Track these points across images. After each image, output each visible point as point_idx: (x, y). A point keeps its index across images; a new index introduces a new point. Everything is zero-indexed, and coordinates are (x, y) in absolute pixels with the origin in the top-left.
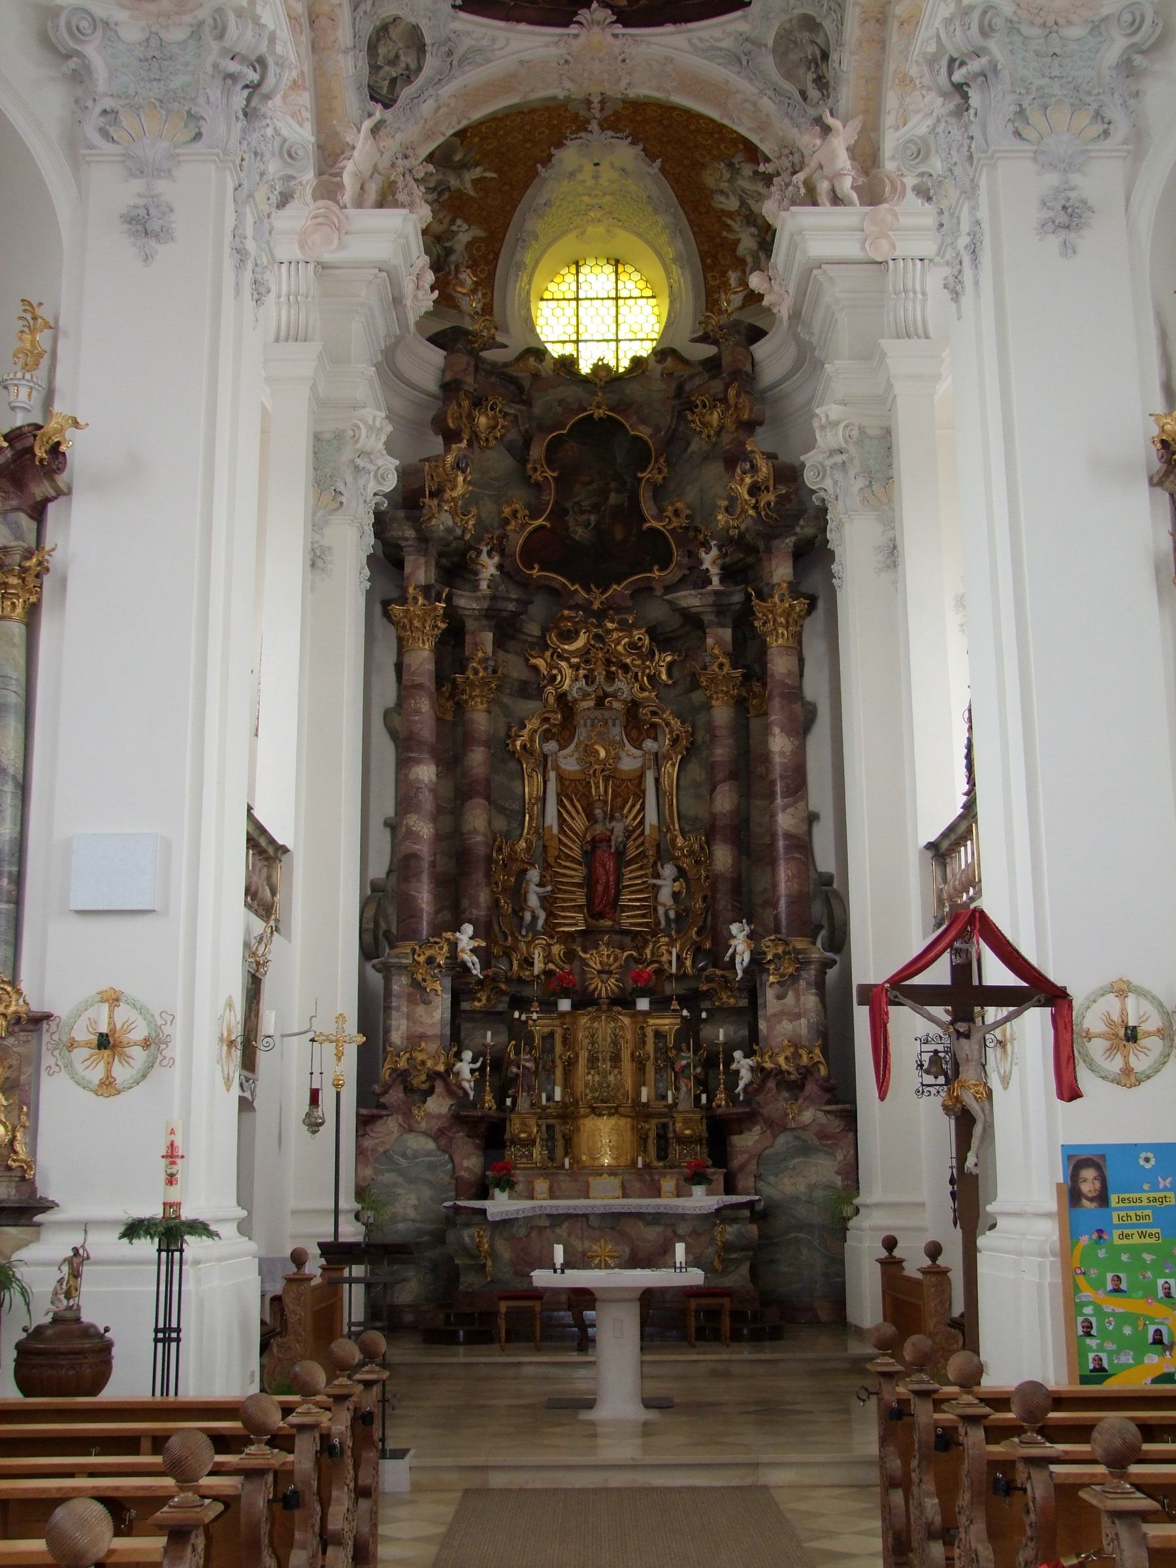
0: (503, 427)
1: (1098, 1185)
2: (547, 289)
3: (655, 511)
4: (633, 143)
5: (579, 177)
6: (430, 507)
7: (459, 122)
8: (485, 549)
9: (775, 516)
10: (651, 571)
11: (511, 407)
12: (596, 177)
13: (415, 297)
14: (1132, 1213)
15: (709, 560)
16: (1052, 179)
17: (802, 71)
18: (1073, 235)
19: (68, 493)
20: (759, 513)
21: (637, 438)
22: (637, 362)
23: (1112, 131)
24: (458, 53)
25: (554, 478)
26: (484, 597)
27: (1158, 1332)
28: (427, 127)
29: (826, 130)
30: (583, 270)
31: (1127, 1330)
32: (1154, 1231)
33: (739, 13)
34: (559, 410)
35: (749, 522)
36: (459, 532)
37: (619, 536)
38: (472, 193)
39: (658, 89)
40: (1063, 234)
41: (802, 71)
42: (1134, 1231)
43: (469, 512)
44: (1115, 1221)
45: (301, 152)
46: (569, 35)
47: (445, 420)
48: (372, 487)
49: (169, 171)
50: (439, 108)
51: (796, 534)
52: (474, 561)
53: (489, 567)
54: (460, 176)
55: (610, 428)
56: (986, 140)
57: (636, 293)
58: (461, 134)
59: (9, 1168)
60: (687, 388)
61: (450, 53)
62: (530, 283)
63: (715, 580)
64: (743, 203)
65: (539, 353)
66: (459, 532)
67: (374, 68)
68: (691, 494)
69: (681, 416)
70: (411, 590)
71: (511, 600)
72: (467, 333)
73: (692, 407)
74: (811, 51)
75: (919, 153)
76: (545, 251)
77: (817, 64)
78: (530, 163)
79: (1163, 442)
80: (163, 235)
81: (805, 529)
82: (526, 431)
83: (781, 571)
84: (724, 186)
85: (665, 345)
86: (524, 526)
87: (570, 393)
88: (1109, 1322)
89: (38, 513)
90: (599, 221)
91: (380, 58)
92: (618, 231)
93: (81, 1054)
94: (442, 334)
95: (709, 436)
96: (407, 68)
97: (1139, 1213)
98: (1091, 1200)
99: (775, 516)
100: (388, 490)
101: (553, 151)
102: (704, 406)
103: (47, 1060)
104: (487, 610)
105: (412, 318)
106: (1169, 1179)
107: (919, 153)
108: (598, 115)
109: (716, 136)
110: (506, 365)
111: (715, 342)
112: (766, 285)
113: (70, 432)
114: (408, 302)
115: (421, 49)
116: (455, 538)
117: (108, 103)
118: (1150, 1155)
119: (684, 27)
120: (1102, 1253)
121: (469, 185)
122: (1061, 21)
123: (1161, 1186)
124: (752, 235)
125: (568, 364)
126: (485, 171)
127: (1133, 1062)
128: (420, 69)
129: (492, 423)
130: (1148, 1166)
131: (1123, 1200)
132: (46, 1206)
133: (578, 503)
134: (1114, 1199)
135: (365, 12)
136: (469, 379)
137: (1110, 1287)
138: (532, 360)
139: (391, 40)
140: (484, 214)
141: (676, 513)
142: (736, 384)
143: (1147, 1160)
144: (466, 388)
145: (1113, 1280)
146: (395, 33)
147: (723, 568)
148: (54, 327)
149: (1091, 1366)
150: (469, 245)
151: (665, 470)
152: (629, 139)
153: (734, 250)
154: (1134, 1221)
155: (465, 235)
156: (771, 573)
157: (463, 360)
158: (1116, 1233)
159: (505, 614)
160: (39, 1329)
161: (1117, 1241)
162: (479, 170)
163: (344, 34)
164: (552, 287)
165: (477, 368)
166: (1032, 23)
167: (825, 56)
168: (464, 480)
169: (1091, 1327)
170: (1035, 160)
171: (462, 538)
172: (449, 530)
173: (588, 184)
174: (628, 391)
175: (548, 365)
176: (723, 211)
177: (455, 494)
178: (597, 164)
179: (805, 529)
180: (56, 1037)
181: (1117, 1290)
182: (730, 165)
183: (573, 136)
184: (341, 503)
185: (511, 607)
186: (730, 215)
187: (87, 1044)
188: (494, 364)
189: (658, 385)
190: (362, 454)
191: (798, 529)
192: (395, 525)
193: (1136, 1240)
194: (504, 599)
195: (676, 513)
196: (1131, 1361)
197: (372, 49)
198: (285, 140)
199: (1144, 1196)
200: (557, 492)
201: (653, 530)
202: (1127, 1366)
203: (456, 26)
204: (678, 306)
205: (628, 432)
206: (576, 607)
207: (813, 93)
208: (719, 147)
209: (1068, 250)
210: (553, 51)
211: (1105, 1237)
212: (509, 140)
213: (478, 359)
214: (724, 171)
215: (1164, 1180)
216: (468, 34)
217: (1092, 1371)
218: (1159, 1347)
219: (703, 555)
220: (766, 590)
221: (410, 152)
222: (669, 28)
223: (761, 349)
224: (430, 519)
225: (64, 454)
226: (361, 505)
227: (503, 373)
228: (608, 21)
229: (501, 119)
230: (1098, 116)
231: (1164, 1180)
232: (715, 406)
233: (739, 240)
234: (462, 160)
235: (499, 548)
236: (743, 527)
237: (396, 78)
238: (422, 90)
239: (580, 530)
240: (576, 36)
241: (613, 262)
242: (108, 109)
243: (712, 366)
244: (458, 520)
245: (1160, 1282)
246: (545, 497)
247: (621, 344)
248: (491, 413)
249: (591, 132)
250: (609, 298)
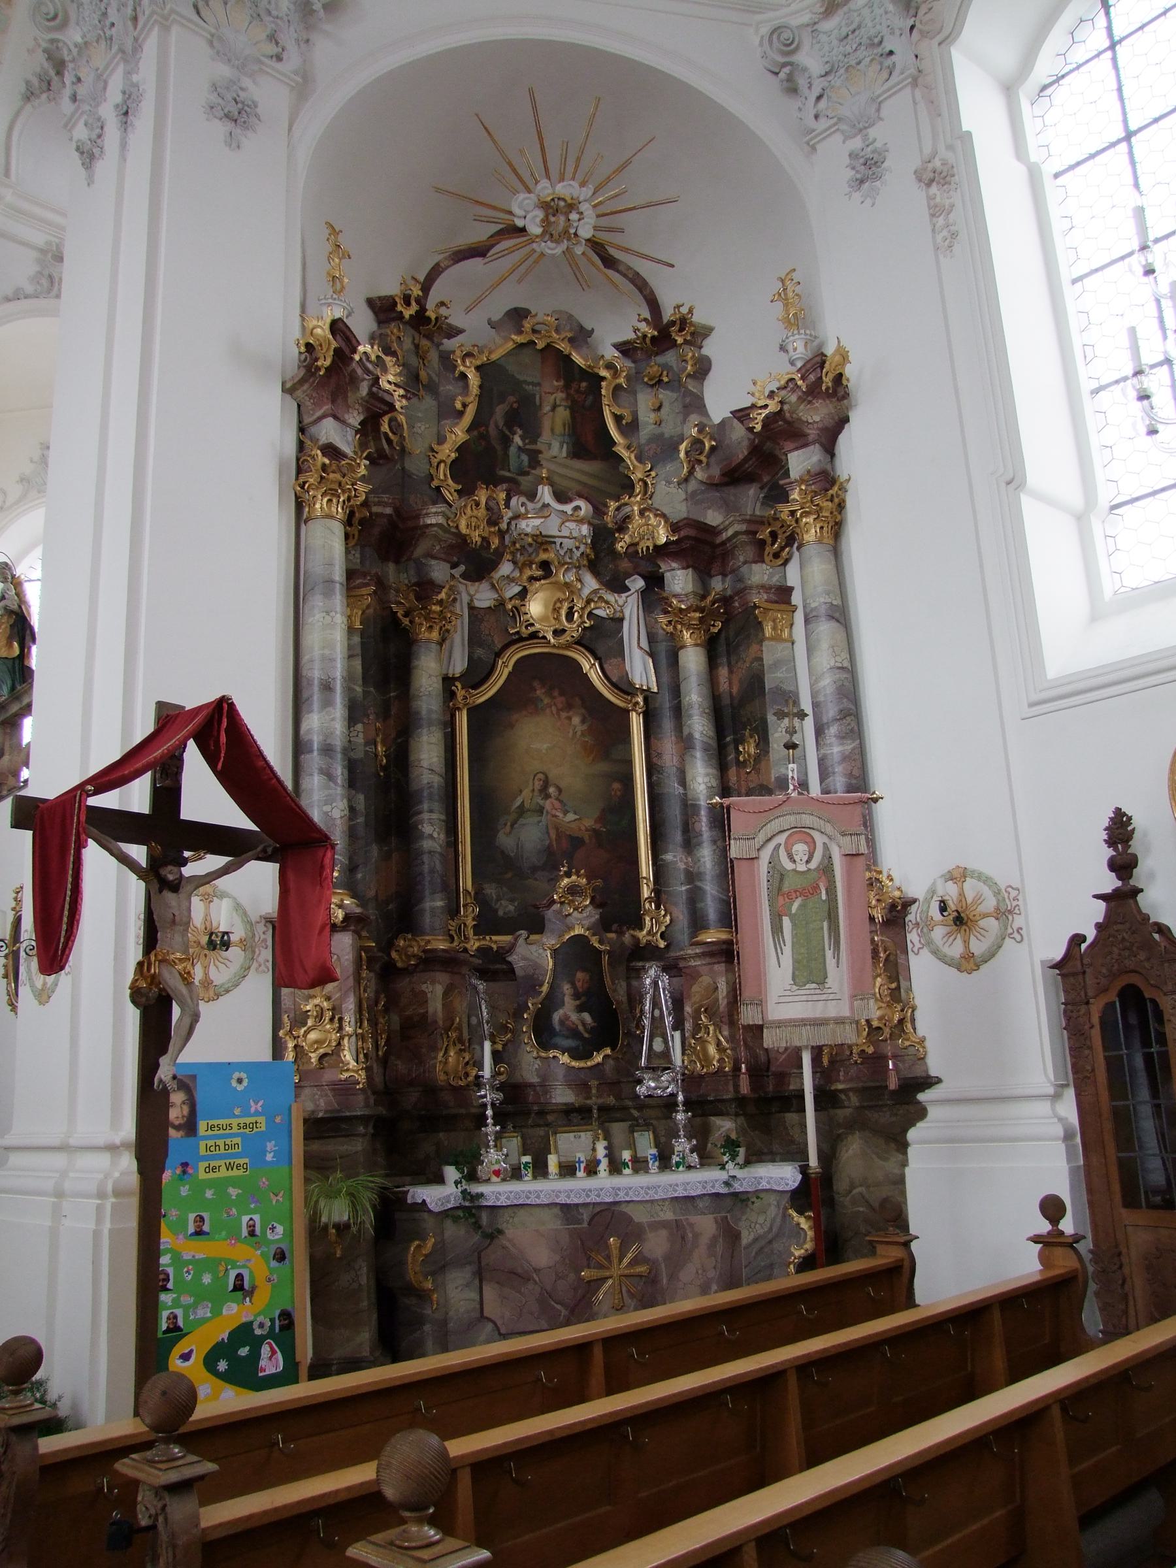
1: (186, 1110)
14: (220, 1142)
18: (239, 131)
23: (285, 56)
27: (239, 1277)
31: (207, 1279)
32: (241, 1161)
40: (230, 125)
42: (222, 1163)
44: (202, 1152)
79: (309, 346)
88: (188, 1272)
97: (228, 1141)
98: (178, 1128)
106: (260, 1103)
118: (243, 1075)
120: (184, 1191)
123: (253, 1110)
127: (213, 974)
130: (240, 1088)
131: (212, 1127)
134: (202, 1126)
137: (191, 1229)
143: (240, 1081)
145: (195, 1221)
149: (164, 1327)
154: (222, 1151)
158: (203, 1165)
161: (202, 1175)
169: (168, 1280)
170: (211, 44)
181: (199, 1233)
193: (223, 1173)
196: (209, 1315)
199: (235, 1122)
202: (204, 1320)
209: (232, 142)
211: (190, 1171)
215: (256, 1103)
217: (165, 1332)
218: (239, 1294)
230: (273, 38)
231: (256, 1103)
245: (245, 1219)
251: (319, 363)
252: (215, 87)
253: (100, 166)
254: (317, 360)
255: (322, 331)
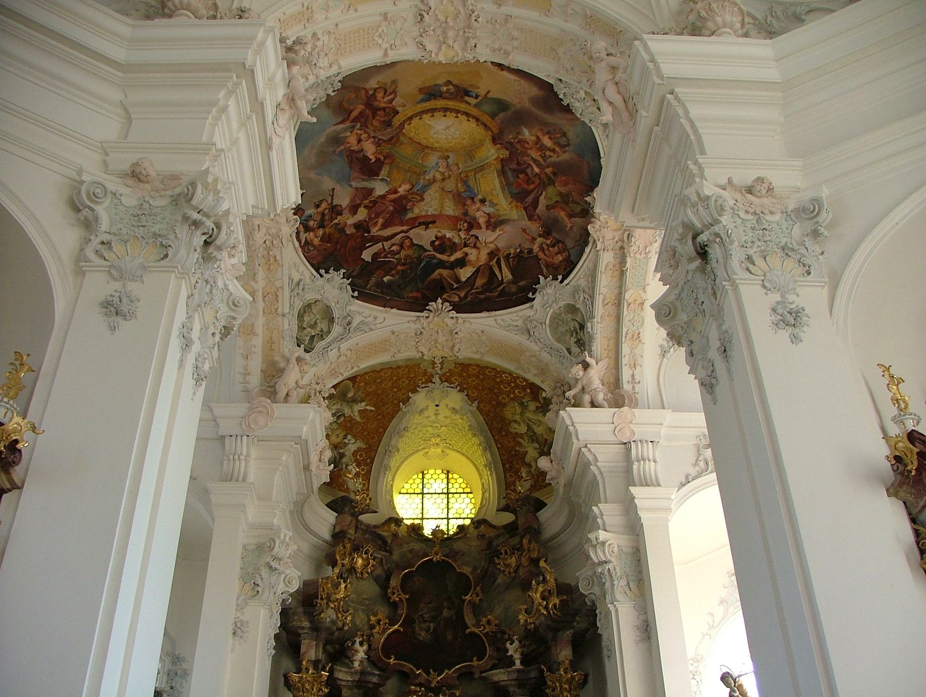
0: (372, 566)
2: (403, 487)
3: (474, 622)
4: (460, 391)
5: (426, 413)
6: (321, 605)
7: (352, 369)
8: (358, 640)
9: (559, 614)
10: (472, 661)
11: (379, 553)
12: (436, 414)
13: (318, 467)
15: (513, 649)
16: (776, 297)
17: (567, 337)
19: (20, 488)
20: (548, 612)
21: (461, 574)
22: (461, 528)
24: (354, 324)
25: (407, 600)
26: (356, 673)
28: (332, 367)
29: (586, 366)
30: (426, 476)
33: (528, 305)
34: (410, 556)
35: (543, 618)
36: (340, 624)
37: (449, 637)
38: (358, 419)
39: (477, 352)
40: (790, 329)
41: (567, 337)
43: (348, 611)
45: (241, 302)
46: (423, 317)
47: (334, 555)
48: (281, 587)
49: (142, 276)
50: (340, 355)
51: (573, 627)
52: (351, 648)
53: (360, 653)
54: (351, 407)
55: (444, 567)
56: (728, 274)
57: (461, 490)
58: (353, 379)
60: (495, 543)
61: (349, 323)
62: (393, 480)
63: (518, 662)
64: (529, 427)
65: (398, 521)
66: (340, 624)
67: (301, 328)
68: (498, 611)
69: (491, 561)
70: (304, 663)
71: (374, 674)
72: (352, 501)
73: (497, 554)
74: (574, 325)
75: (669, 314)
76: (402, 462)
77: (577, 333)
78: (396, 402)
79: (896, 458)
81: (580, 624)
82: (388, 569)
83: (564, 654)
84: (517, 417)
85: (481, 517)
86: (385, 630)
87: (416, 546)
90: (438, 445)
91: (305, 323)
92: (448, 451)
94: (333, 501)
95: (510, 573)
96: (322, 331)
99: (559, 614)
100: (292, 591)
101: (410, 395)
102: (506, 553)
104: (358, 681)
105: (316, 485)
107: (669, 314)
108: (439, 372)
109: (513, 385)
110: (375, 527)
111: (514, 511)
112: (549, 465)
114: (313, 468)
115: (332, 320)
116: (337, 629)
117: (106, 238)
119: (493, 313)
121: (356, 414)
122: (766, 212)
124: (536, 449)
125: (416, 529)
126: (367, 405)
128: (329, 332)
129: (365, 563)
133: (422, 616)
135: (298, 294)
136: (352, 531)
138: (393, 525)
139: (313, 313)
140: (366, 433)
141: (489, 622)
142: (528, 536)
144: (349, 536)
146: (315, 309)
147: (522, 654)
150: (355, 453)
151: (481, 595)
152: (458, 388)
153: (523, 459)
155: (353, 445)
156: (557, 655)
157: (348, 518)
159: (370, 686)
162: (363, 404)
163: (284, 305)
164: (407, 486)
165: (357, 528)
166: (747, 212)
167: (582, 327)
168: (346, 587)
171: (342, 629)
172: (334, 622)
173: (431, 419)
174: (455, 547)
175: (402, 531)
176: (517, 433)
177: (338, 597)
178: (437, 406)
179: (580, 624)
182: (522, 404)
183: (424, 386)
184: (258, 592)
185: (375, 680)
186: (521, 436)
188: (368, 526)
189: (474, 543)
190: (275, 558)
191: (575, 624)
192: (296, 618)
194: (370, 674)
195: (489, 622)
197: (300, 317)
198: (231, 294)
200: (408, 609)
201: (472, 633)
203: (353, 308)
204: (487, 495)
205: (456, 570)
206: (420, 685)
207: (575, 349)
208: (514, 392)
209: (795, 339)
210: (413, 326)
212: (383, 386)
213: (358, 521)
214: (517, 408)
216: (360, 313)
219: (508, 645)
220: (555, 667)
221: (320, 381)
222: (485, 314)
223: (543, 515)
224: (320, 614)
225: (20, 451)
226: (272, 594)
227: (375, 533)
228: (447, 310)
229: (378, 372)
232: (513, 553)
233: (527, 452)
234: (354, 396)
235: (368, 640)
236: (537, 622)
237: (314, 336)
238: (329, 344)
239: (423, 634)
240: (427, 317)
241: (445, 472)
242: (105, 241)
243: (511, 528)
244: (340, 615)
246: (399, 612)
247: (450, 521)
248: (364, 556)
249: (434, 383)
250: (442, 493)
251: (909, 468)
252: (774, 310)
253: (718, 389)
254: (906, 466)
255: (904, 444)
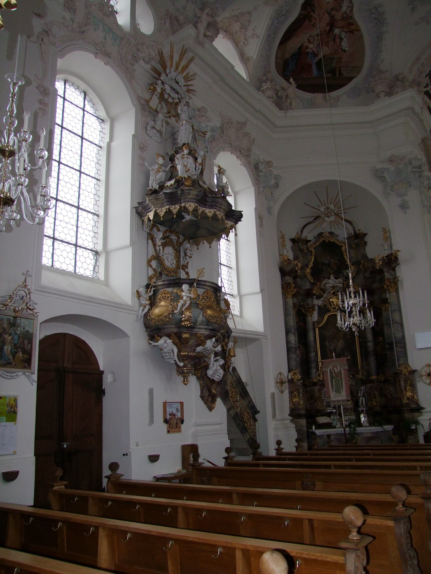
59: (414, 401)
80: (408, 207)
89: (394, 269)
93: (424, 378)
103: (417, 379)
113: (399, 253)
132: (423, 408)
148: (389, 232)
160: (427, 432)
180: (418, 374)
187: (425, 375)
